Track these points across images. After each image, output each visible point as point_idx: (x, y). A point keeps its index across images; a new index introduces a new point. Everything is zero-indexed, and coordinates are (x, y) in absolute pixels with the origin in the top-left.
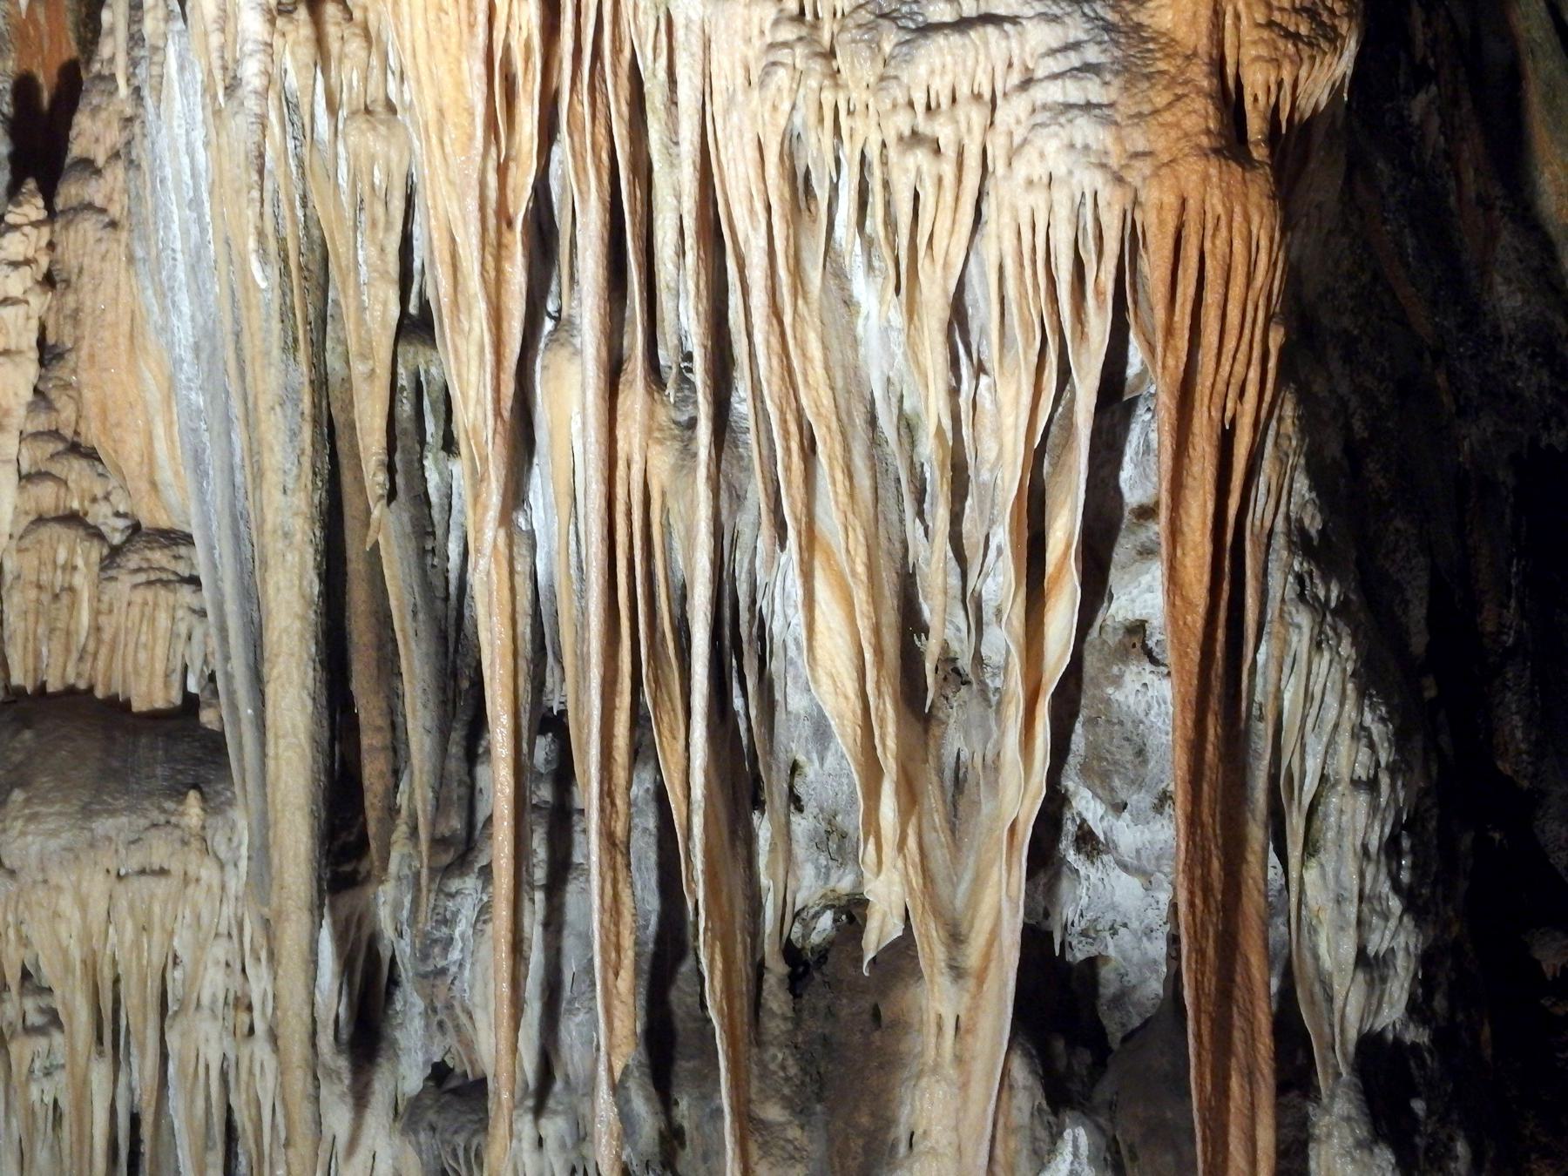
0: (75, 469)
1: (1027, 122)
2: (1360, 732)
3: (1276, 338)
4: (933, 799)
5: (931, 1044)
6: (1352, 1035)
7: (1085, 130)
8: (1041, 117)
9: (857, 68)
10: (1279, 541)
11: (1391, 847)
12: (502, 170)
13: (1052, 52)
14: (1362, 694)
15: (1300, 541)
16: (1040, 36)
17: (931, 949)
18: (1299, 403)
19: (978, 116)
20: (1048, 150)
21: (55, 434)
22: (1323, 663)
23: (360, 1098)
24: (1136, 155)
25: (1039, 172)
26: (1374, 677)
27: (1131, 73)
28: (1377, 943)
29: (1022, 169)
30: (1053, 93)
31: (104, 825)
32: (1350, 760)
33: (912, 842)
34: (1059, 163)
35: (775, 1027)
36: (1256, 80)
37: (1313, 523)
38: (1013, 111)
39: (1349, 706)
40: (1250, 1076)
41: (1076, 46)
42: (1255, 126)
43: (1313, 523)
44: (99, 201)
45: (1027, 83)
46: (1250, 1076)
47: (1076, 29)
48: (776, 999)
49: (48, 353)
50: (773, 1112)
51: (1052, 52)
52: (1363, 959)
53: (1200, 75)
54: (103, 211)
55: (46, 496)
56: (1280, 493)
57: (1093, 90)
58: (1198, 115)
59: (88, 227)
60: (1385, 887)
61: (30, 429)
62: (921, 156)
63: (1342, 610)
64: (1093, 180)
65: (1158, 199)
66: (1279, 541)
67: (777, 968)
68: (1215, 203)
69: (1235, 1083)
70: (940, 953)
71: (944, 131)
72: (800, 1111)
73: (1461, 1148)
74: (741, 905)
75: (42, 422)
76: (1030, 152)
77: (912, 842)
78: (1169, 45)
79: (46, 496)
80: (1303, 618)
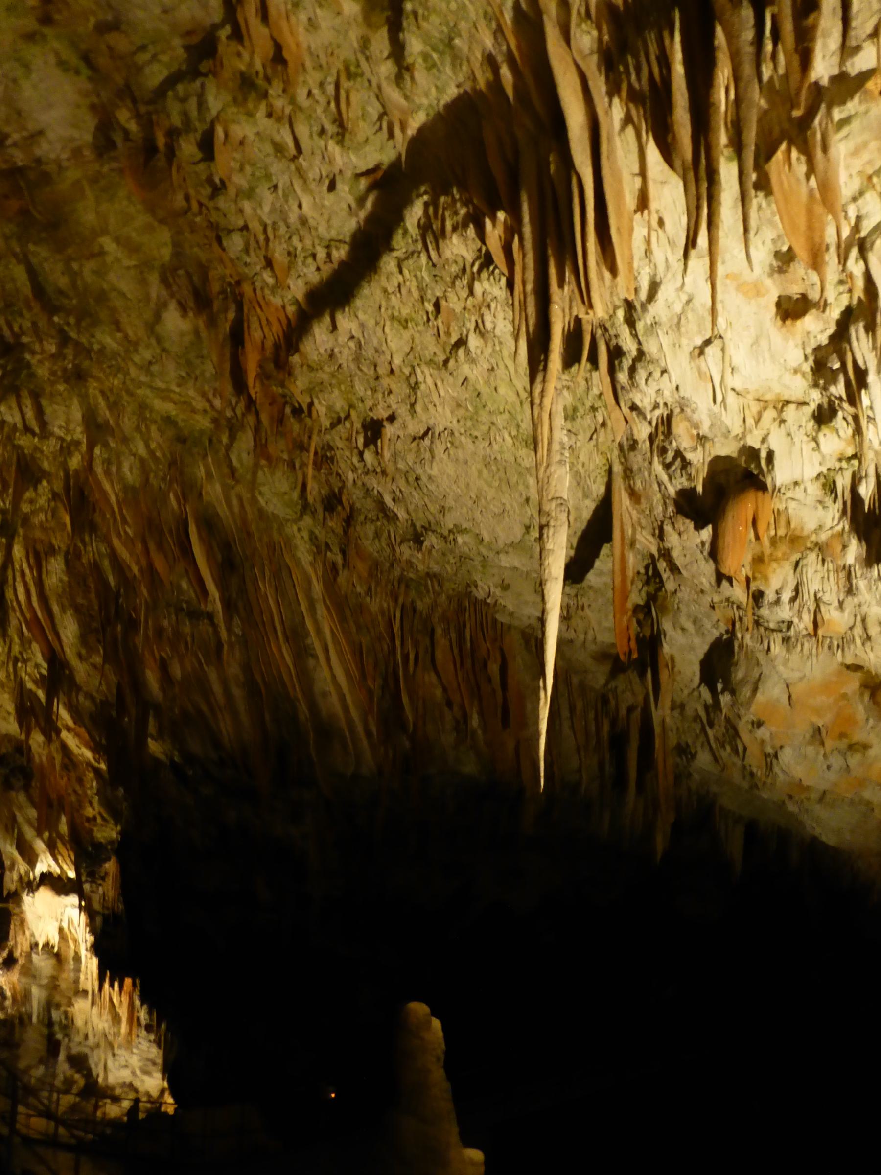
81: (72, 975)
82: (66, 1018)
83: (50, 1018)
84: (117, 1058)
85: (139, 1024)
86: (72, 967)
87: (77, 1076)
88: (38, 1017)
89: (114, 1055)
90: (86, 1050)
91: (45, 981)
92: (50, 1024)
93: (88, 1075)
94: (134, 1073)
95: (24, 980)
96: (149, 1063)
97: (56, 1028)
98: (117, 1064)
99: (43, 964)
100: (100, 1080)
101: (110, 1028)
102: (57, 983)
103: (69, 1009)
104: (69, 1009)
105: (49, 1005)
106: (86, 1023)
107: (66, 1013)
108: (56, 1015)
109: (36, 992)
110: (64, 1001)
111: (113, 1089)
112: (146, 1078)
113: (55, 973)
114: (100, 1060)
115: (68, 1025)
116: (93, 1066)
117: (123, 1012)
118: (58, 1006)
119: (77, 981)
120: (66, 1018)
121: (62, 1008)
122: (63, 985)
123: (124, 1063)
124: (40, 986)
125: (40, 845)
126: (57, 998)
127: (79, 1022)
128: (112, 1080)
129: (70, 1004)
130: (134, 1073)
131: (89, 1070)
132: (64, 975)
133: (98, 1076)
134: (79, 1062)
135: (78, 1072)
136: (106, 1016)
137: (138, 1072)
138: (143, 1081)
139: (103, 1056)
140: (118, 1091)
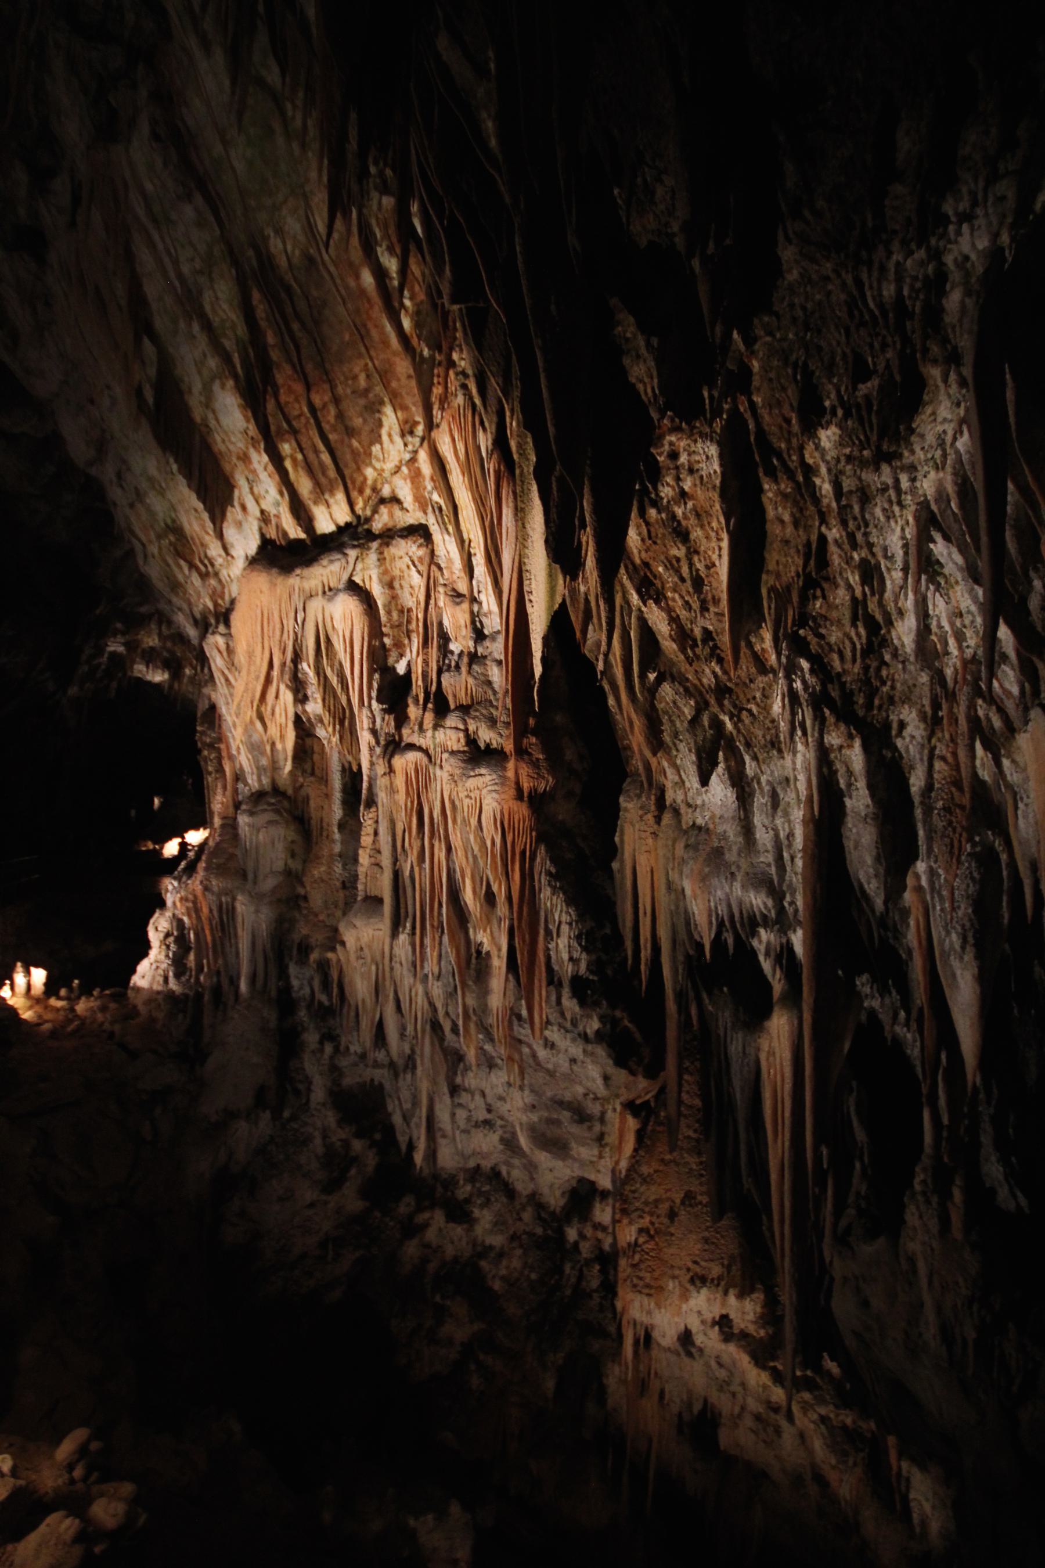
0: (378, 855)
2: (568, 913)
3: (534, 834)
4: (495, 922)
5: (495, 971)
6: (570, 974)
7: (494, 795)
9: (460, 784)
10: (543, 874)
11: (578, 938)
12: (412, 802)
14: (568, 905)
15: (549, 873)
16: (489, 778)
17: (494, 953)
18: (546, 846)
22: (555, 898)
23: (415, 975)
26: (569, 902)
27: (503, 784)
28: (575, 955)
30: (489, 788)
31: (372, 920)
32: (565, 918)
33: (488, 930)
34: (491, 801)
35: (473, 967)
36: (526, 785)
37: (553, 870)
38: (484, 791)
39: (564, 908)
40: (540, 981)
42: (526, 794)
43: (553, 870)
46: (540, 981)
47: (494, 777)
48: (474, 961)
49: (376, 833)
50: (470, 983)
52: (571, 959)
53: (513, 785)
55: (373, 860)
56: (542, 864)
57: (496, 787)
58: (512, 792)
60: (576, 945)
62: (468, 800)
63: (561, 888)
65: (506, 807)
66: (543, 874)
67: (474, 955)
68: (516, 809)
69: (536, 981)
70: (496, 953)
71: (472, 795)
72: (475, 982)
73: (604, 1002)
74: (463, 941)
77: (488, 930)
78: (509, 778)
79: (373, 860)
80: (549, 889)
81: (338, 868)
82: (326, 985)
83: (286, 990)
84: (464, 1098)
85: (553, 980)
86: (337, 848)
87: (357, 1145)
88: (253, 980)
89: (454, 1090)
90: (381, 1075)
91: (269, 884)
92: (286, 1003)
93: (385, 1139)
94: (510, 1143)
95: (215, 883)
96: (565, 1115)
97: (302, 1014)
98: (461, 1114)
99: (265, 838)
100: (418, 1157)
101: (451, 995)
102: (301, 891)
103: (330, 955)
104: (330, 955)
105: (283, 947)
106: (377, 990)
107: (323, 967)
108: (301, 980)
109: (242, 906)
110: (318, 937)
111: (450, 1182)
112: (543, 1158)
113: (295, 865)
114: (415, 1103)
115: (333, 1005)
116: (397, 1119)
117: (491, 939)
118: (305, 949)
119: (350, 883)
120: (326, 985)
121: (314, 956)
122: (317, 899)
123: (482, 1115)
124: (257, 898)
125: (231, 420)
126: (303, 929)
127: (361, 988)
128: (447, 1158)
129: (335, 940)
130: (510, 1143)
131: (389, 1130)
132: (318, 871)
133: (411, 1147)
134: (364, 1108)
135: (359, 1135)
136: (440, 955)
137: (523, 1141)
138: (531, 1167)
139: (424, 1086)
140: (464, 1190)
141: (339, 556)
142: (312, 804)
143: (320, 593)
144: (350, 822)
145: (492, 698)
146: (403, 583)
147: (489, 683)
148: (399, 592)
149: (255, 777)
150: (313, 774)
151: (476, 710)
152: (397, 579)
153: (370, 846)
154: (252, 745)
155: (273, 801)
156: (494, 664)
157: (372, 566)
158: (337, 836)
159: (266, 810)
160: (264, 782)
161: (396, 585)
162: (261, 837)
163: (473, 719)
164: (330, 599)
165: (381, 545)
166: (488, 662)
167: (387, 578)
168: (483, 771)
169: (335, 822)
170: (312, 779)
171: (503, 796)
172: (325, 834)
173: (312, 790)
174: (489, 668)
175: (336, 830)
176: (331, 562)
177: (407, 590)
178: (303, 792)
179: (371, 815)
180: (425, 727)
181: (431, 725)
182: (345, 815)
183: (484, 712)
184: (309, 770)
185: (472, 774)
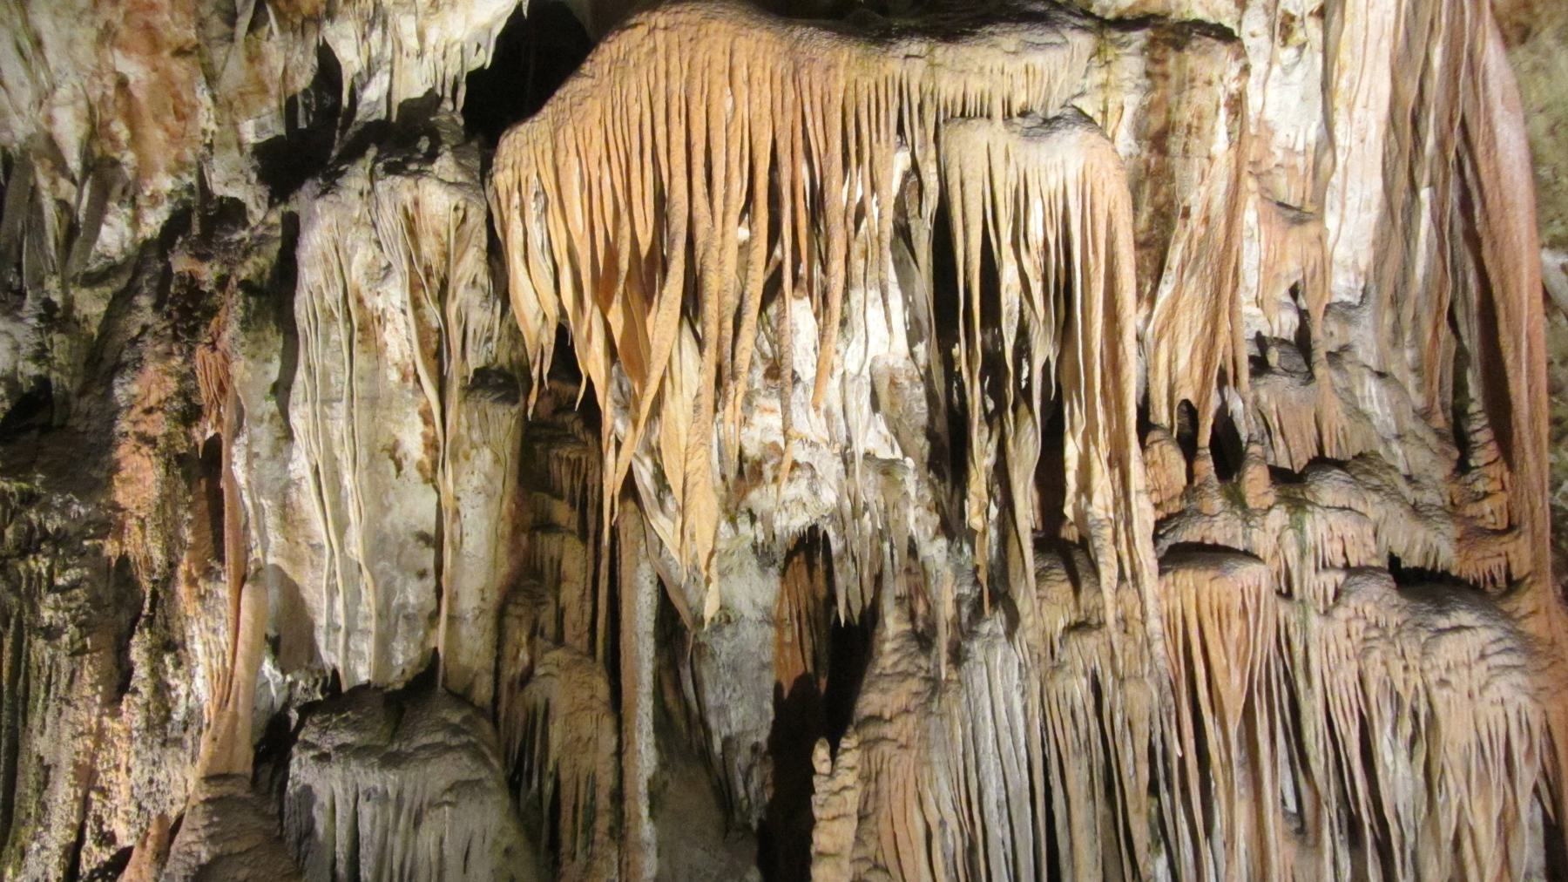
1: (1486, 675)
7: (1517, 678)
8: (1494, 672)
13: (1493, 642)
16: (1485, 635)
19: (1465, 672)
20: (1503, 687)
21: (866, 859)
24: (1541, 689)
25: (1497, 697)
29: (1488, 695)
34: (1506, 692)
41: (1500, 640)
44: (890, 735)
45: (1483, 656)
49: (862, 817)
51: (1493, 642)
54: (895, 740)
59: (887, 748)
61: (855, 856)
64: (1524, 700)
75: (861, 853)
76: (1493, 688)
141: (1058, 40)
142: (557, 734)
143: (998, 112)
144: (671, 788)
145: (1381, 451)
146: (1194, 143)
147: (1366, 417)
148: (1178, 162)
149: (368, 646)
150: (559, 641)
151: (1367, 472)
152: (1181, 132)
153: (847, 852)
154: (383, 540)
155: (456, 718)
156: (1366, 371)
157: (1129, 85)
158: (646, 830)
159: (446, 748)
160: (400, 659)
161: (1175, 144)
162: (427, 838)
163: (1377, 489)
164: (1028, 135)
165: (1152, 43)
166: (1348, 367)
167: (1156, 122)
168: (1464, 617)
169: (643, 787)
170: (558, 654)
171: (1540, 681)
172: (603, 823)
173: (567, 691)
174: (1356, 381)
175: (645, 812)
176: (1037, 46)
177: (1197, 163)
178: (534, 693)
179: (847, 759)
180: (1251, 503)
181: (1270, 499)
182: (663, 765)
183: (1386, 477)
184: (550, 630)
185: (1443, 623)
